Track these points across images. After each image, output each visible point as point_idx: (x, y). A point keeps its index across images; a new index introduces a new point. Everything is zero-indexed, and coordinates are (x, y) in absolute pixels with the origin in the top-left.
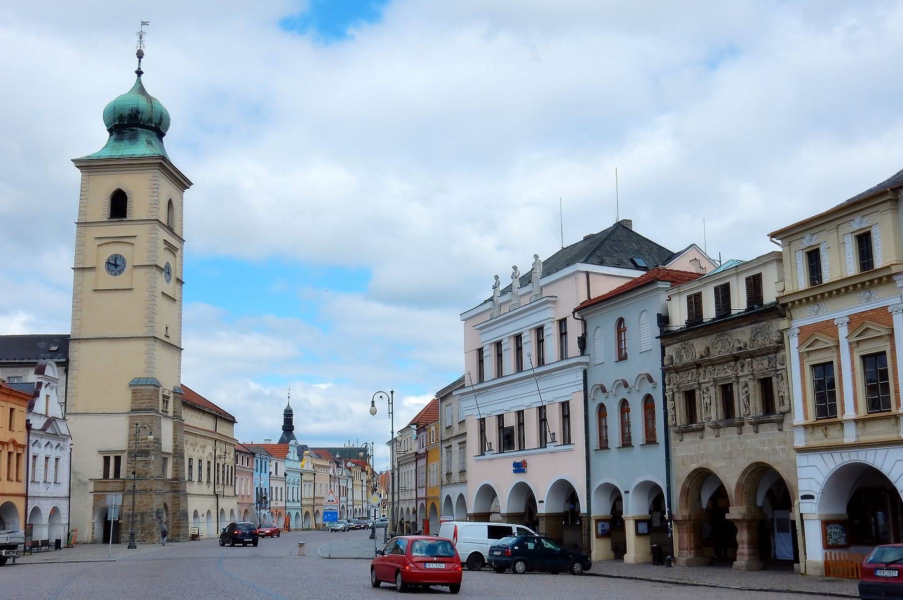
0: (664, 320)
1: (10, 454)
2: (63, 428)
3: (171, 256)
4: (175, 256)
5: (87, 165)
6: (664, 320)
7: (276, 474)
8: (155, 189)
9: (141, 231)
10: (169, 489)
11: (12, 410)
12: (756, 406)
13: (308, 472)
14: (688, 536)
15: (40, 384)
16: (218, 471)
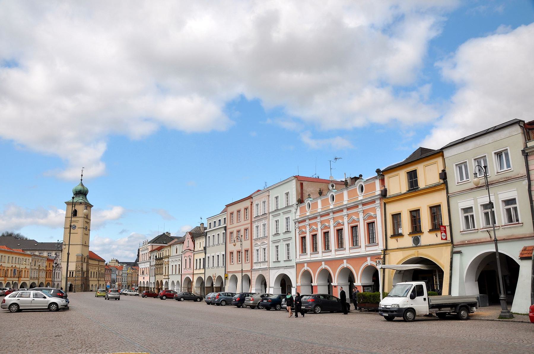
0: (156, 257)
1: (49, 272)
5: (68, 203)
6: (156, 257)
7: (119, 274)
11: (50, 263)
13: (130, 274)
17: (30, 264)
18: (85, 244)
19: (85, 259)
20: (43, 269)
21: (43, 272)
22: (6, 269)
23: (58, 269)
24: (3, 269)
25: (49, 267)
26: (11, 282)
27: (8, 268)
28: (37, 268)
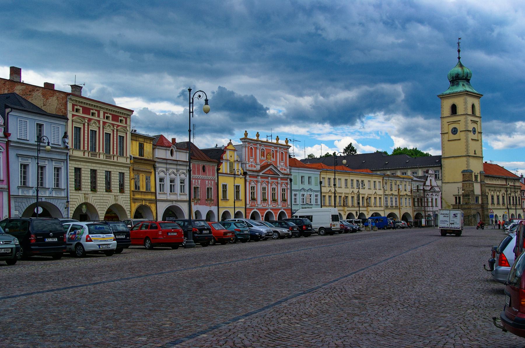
2: (437, 189)
3: (476, 125)
4: (477, 124)
8: (466, 103)
9: (462, 118)
10: (480, 207)
15: (428, 176)
16: (510, 200)
17: (382, 188)
18: (475, 154)
19: (476, 177)
20: (407, 195)
21: (408, 199)
22: (343, 195)
24: (340, 197)
26: (354, 213)
27: (346, 195)
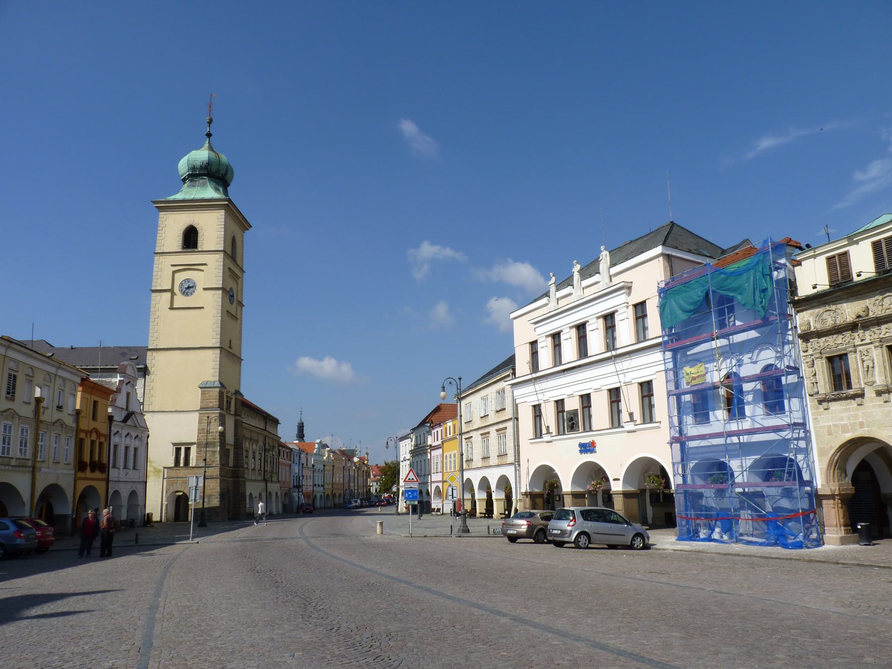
1: (93, 442)
4: (237, 284)
7: (307, 465)
11: (95, 403)
12: (824, 386)
14: (837, 511)
18: (230, 347)
19: (229, 403)
20: (63, 425)
23: (134, 434)
25: (94, 418)
28: (27, 411)
